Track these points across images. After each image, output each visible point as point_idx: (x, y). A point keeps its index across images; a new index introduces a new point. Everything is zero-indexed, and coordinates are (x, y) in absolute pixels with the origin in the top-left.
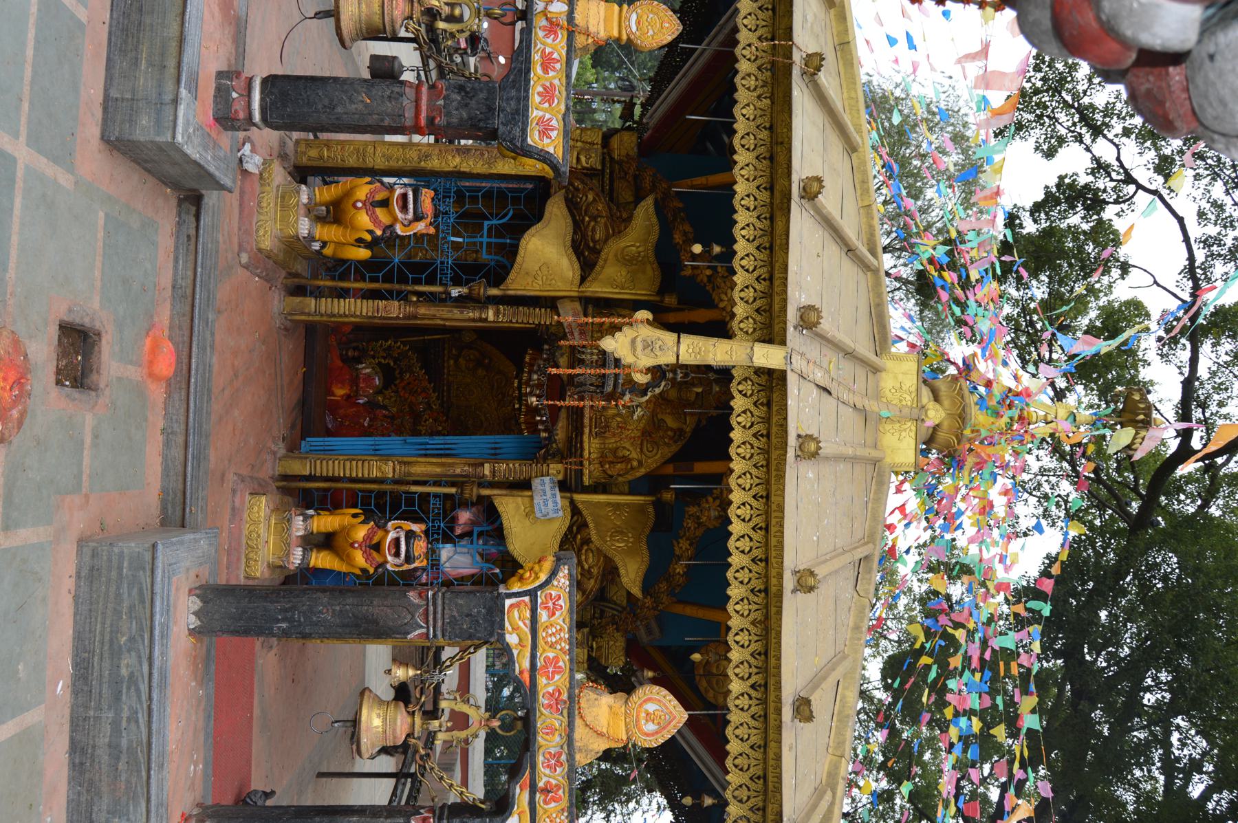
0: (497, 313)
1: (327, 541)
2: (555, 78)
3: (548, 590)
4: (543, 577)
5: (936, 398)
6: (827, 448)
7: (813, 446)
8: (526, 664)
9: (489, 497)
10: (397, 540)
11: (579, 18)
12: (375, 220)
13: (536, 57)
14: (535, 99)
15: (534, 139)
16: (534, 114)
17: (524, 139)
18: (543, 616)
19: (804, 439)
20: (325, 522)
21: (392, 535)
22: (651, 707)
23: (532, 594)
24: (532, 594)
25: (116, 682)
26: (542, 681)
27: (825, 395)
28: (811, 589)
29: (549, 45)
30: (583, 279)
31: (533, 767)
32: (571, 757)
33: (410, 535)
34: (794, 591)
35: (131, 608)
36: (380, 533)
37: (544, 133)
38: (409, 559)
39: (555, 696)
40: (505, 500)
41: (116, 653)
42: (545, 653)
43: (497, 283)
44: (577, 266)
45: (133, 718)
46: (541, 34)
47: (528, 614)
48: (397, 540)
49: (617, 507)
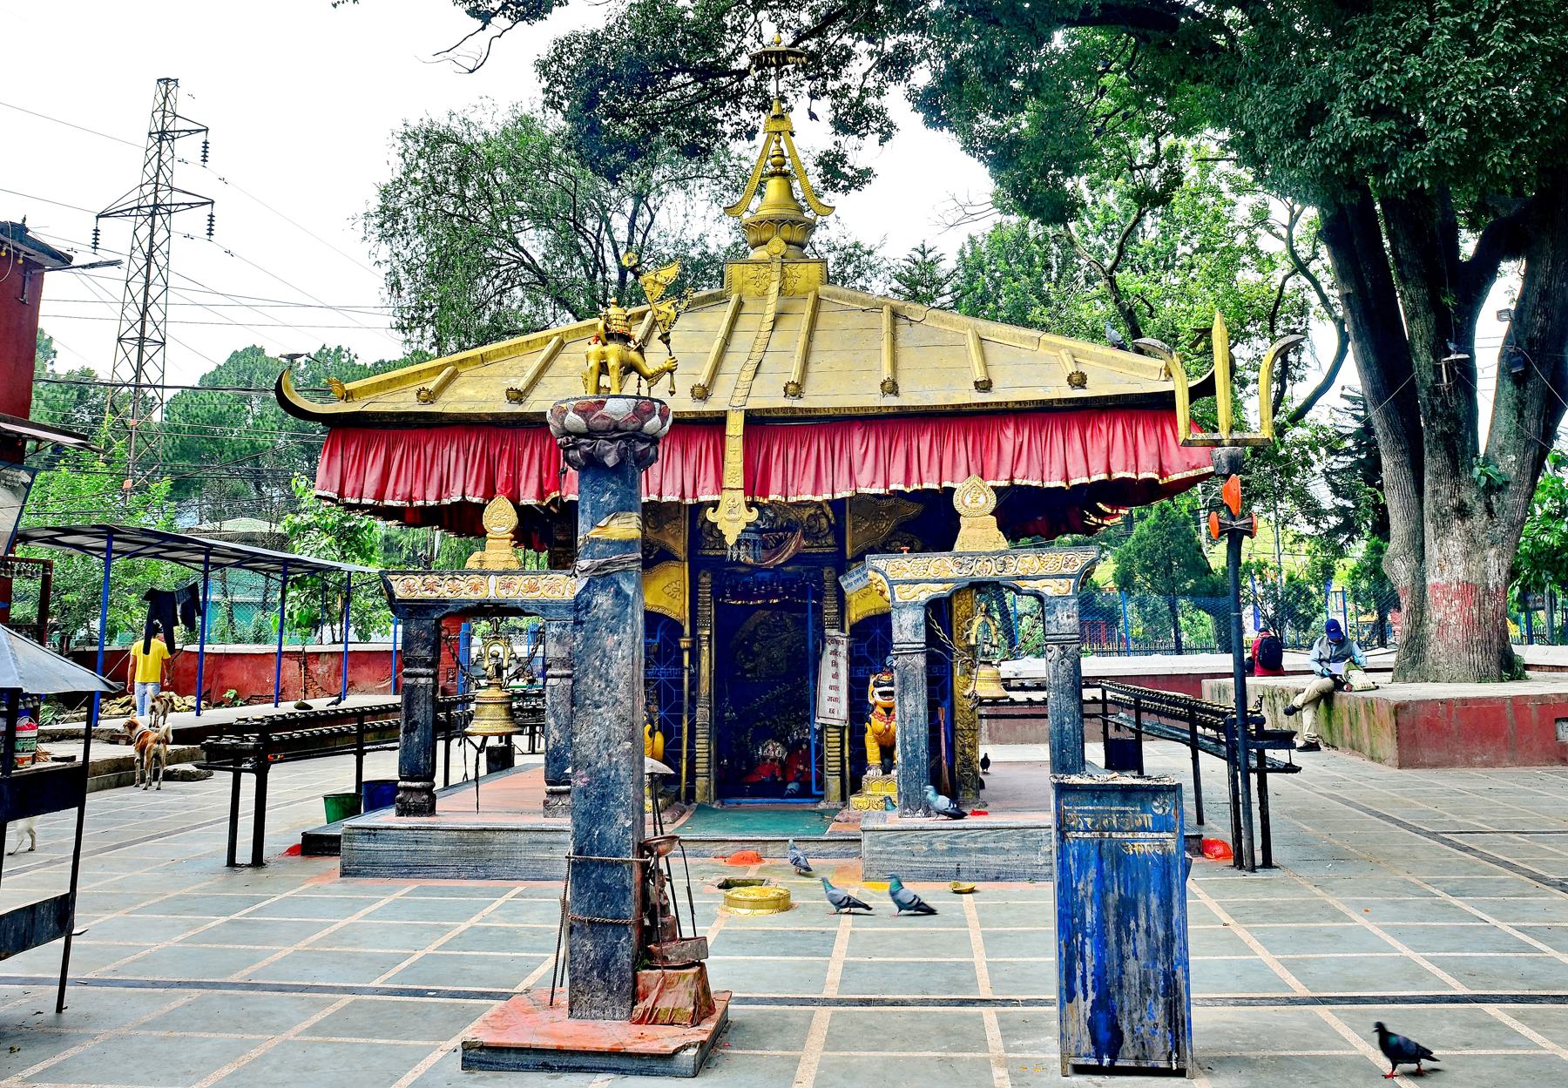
0: (704, 628)
1: (887, 751)
2: (543, 581)
3: (888, 573)
4: (880, 577)
5: (765, 243)
6: (795, 378)
8: (940, 586)
9: (852, 628)
10: (881, 694)
11: (500, 568)
14: (557, 596)
18: (908, 576)
20: (873, 753)
21: (878, 698)
22: (968, 500)
23: (892, 584)
24: (892, 584)
25: (951, 851)
26: (951, 575)
27: (762, 370)
28: (895, 384)
30: (676, 559)
31: (1009, 578)
32: (1001, 553)
33: (877, 685)
34: (897, 394)
35: (904, 844)
36: (879, 710)
38: (891, 684)
39: (961, 565)
40: (853, 617)
41: (933, 852)
42: (932, 573)
43: (682, 629)
44: (664, 564)
46: (512, 594)
47: (906, 587)
48: (881, 694)
49: (855, 527)
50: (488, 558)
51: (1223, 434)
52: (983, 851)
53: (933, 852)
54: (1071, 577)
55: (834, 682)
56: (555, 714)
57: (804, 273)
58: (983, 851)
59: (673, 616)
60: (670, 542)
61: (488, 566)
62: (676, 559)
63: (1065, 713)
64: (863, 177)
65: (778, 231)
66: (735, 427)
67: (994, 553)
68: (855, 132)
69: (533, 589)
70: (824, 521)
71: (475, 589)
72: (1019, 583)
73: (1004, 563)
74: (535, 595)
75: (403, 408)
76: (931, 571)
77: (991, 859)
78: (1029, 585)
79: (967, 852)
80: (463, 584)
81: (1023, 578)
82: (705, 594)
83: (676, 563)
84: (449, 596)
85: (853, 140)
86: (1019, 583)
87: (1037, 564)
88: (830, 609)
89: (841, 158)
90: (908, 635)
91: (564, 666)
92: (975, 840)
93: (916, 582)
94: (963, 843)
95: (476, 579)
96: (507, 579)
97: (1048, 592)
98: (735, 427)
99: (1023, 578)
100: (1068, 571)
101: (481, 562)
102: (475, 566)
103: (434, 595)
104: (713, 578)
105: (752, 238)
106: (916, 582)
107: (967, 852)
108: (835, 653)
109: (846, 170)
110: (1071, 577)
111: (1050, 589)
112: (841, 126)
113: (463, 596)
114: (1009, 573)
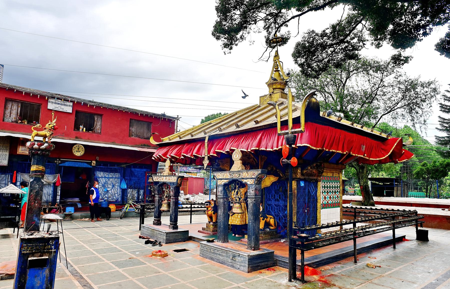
8: (226, 181)
12: (210, 210)
18: (220, 178)
25: (214, 253)
26: (228, 177)
31: (240, 179)
39: (230, 175)
52: (219, 254)
54: (254, 178)
58: (219, 254)
64: (406, 60)
72: (242, 180)
77: (221, 257)
86: (242, 180)
89: (400, 55)
92: (218, 251)
93: (222, 179)
97: (249, 183)
100: (253, 177)
106: (222, 179)
110: (254, 178)
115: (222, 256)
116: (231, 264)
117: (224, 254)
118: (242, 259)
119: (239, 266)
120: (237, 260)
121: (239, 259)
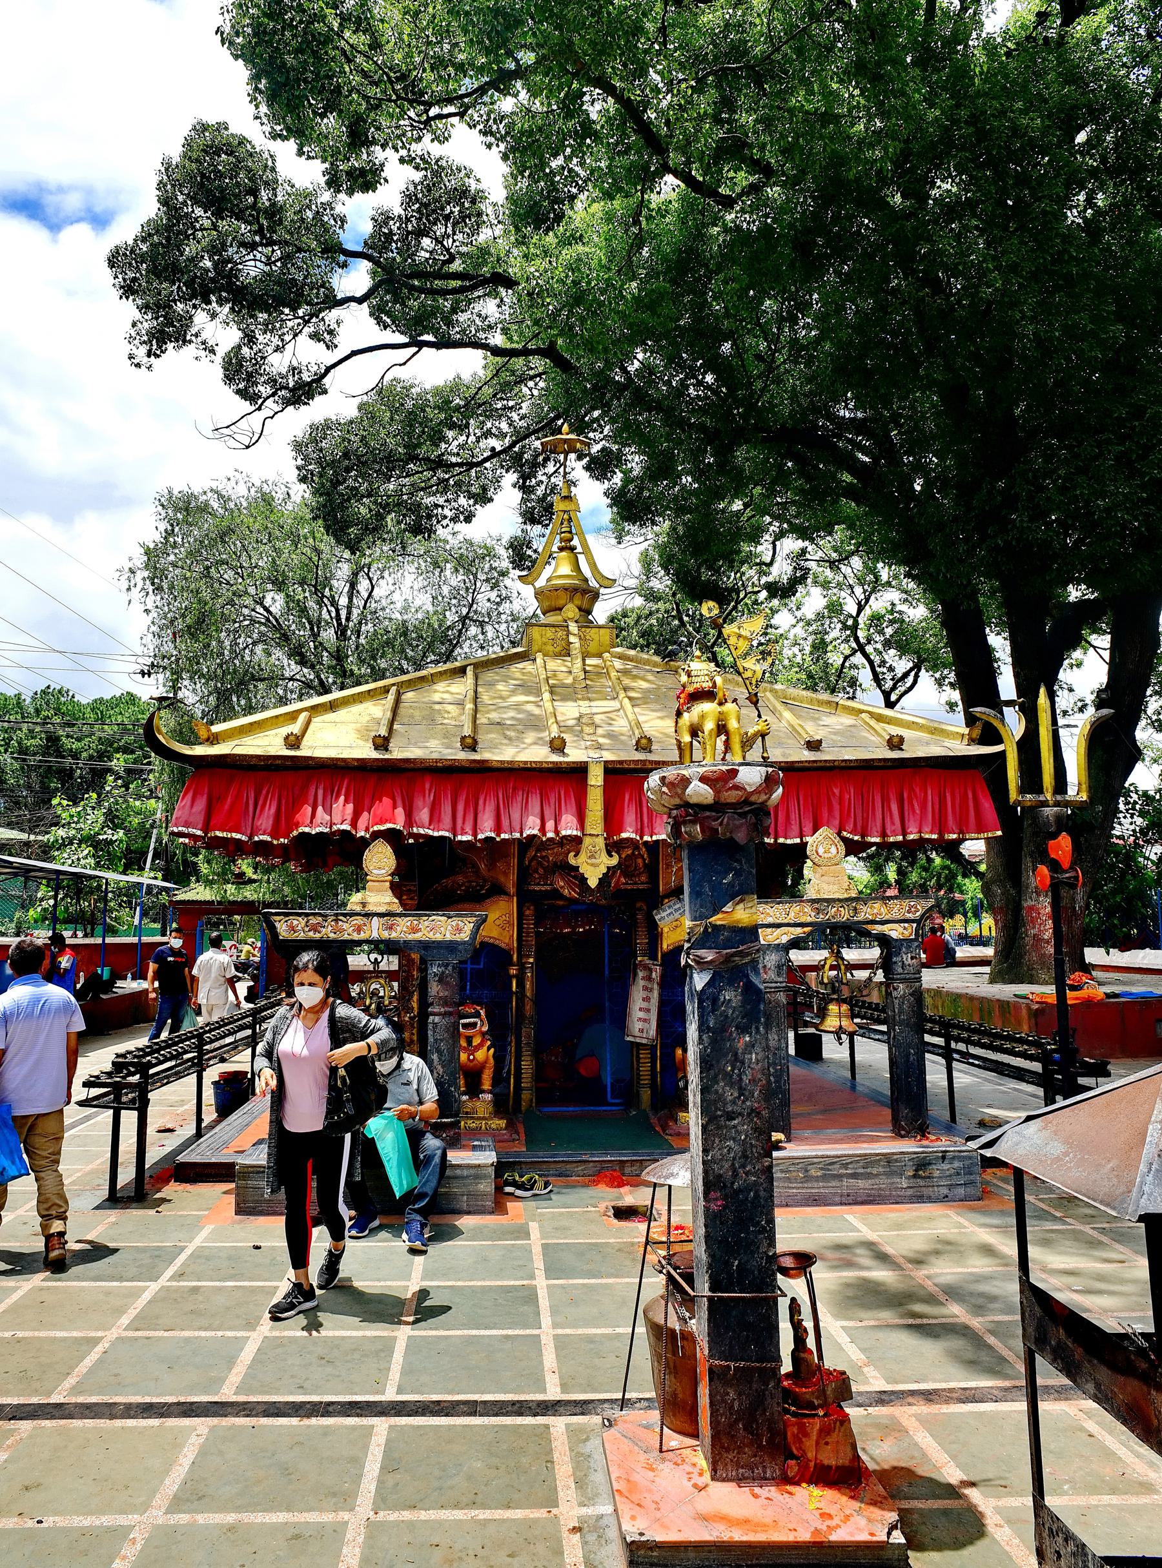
0: (529, 956)
7: (644, 741)
11: (382, 910)
12: (481, 1045)
13: (410, 937)
14: (439, 937)
15: (465, 936)
16: (449, 937)
17: (464, 943)
18: (770, 920)
19: (638, 747)
25: (824, 1178)
26: (809, 920)
29: (403, 930)
30: (506, 893)
37: (460, 930)
39: (818, 911)
40: (665, 946)
44: (494, 899)
45: (845, 1166)
50: (369, 900)
51: (1049, 796)
53: (808, 1178)
54: (913, 921)
55: (645, 1005)
56: (439, 1051)
57: (596, 637)
58: (854, 1176)
59: (503, 945)
60: (502, 879)
61: (371, 908)
62: (506, 893)
63: (909, 1046)
65: (571, 599)
66: (596, 778)
67: (847, 900)
68: (539, 523)
69: (415, 930)
70: (640, 861)
71: (359, 930)
72: (869, 927)
73: (855, 909)
74: (418, 936)
75: (273, 752)
76: (792, 914)
77: (861, 1183)
78: (877, 929)
79: (839, 1177)
80: (345, 926)
81: (873, 922)
82: (530, 925)
83: (503, 897)
84: (332, 936)
85: (538, 529)
86: (869, 927)
87: (884, 910)
88: (642, 941)
90: (772, 975)
91: (445, 1004)
92: (845, 1166)
93: (778, 926)
94: (836, 1170)
95: (359, 920)
96: (391, 920)
97: (894, 935)
98: (596, 778)
99: (873, 922)
100: (910, 916)
101: (364, 904)
102: (358, 908)
103: (318, 936)
104: (536, 910)
105: (546, 604)
106: (778, 926)
107: (839, 1177)
108: (649, 978)
109: (529, 552)
110: (913, 921)
111: (895, 932)
112: (530, 517)
113: (346, 937)
114: (861, 917)
115: (869, 1176)
116: (910, 1192)
117: (875, 1171)
118: (956, 1164)
119: (945, 1191)
120: (937, 1174)
121: (945, 1166)
